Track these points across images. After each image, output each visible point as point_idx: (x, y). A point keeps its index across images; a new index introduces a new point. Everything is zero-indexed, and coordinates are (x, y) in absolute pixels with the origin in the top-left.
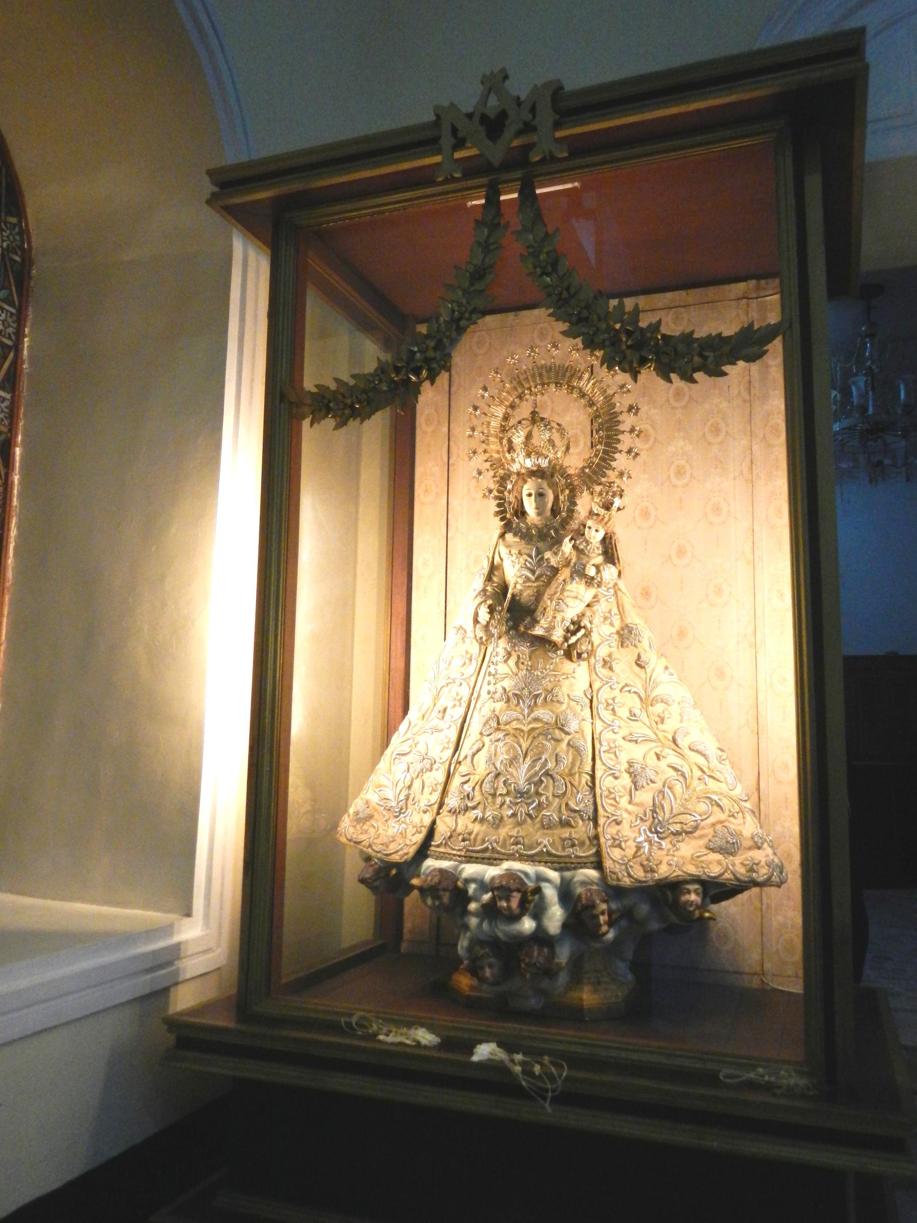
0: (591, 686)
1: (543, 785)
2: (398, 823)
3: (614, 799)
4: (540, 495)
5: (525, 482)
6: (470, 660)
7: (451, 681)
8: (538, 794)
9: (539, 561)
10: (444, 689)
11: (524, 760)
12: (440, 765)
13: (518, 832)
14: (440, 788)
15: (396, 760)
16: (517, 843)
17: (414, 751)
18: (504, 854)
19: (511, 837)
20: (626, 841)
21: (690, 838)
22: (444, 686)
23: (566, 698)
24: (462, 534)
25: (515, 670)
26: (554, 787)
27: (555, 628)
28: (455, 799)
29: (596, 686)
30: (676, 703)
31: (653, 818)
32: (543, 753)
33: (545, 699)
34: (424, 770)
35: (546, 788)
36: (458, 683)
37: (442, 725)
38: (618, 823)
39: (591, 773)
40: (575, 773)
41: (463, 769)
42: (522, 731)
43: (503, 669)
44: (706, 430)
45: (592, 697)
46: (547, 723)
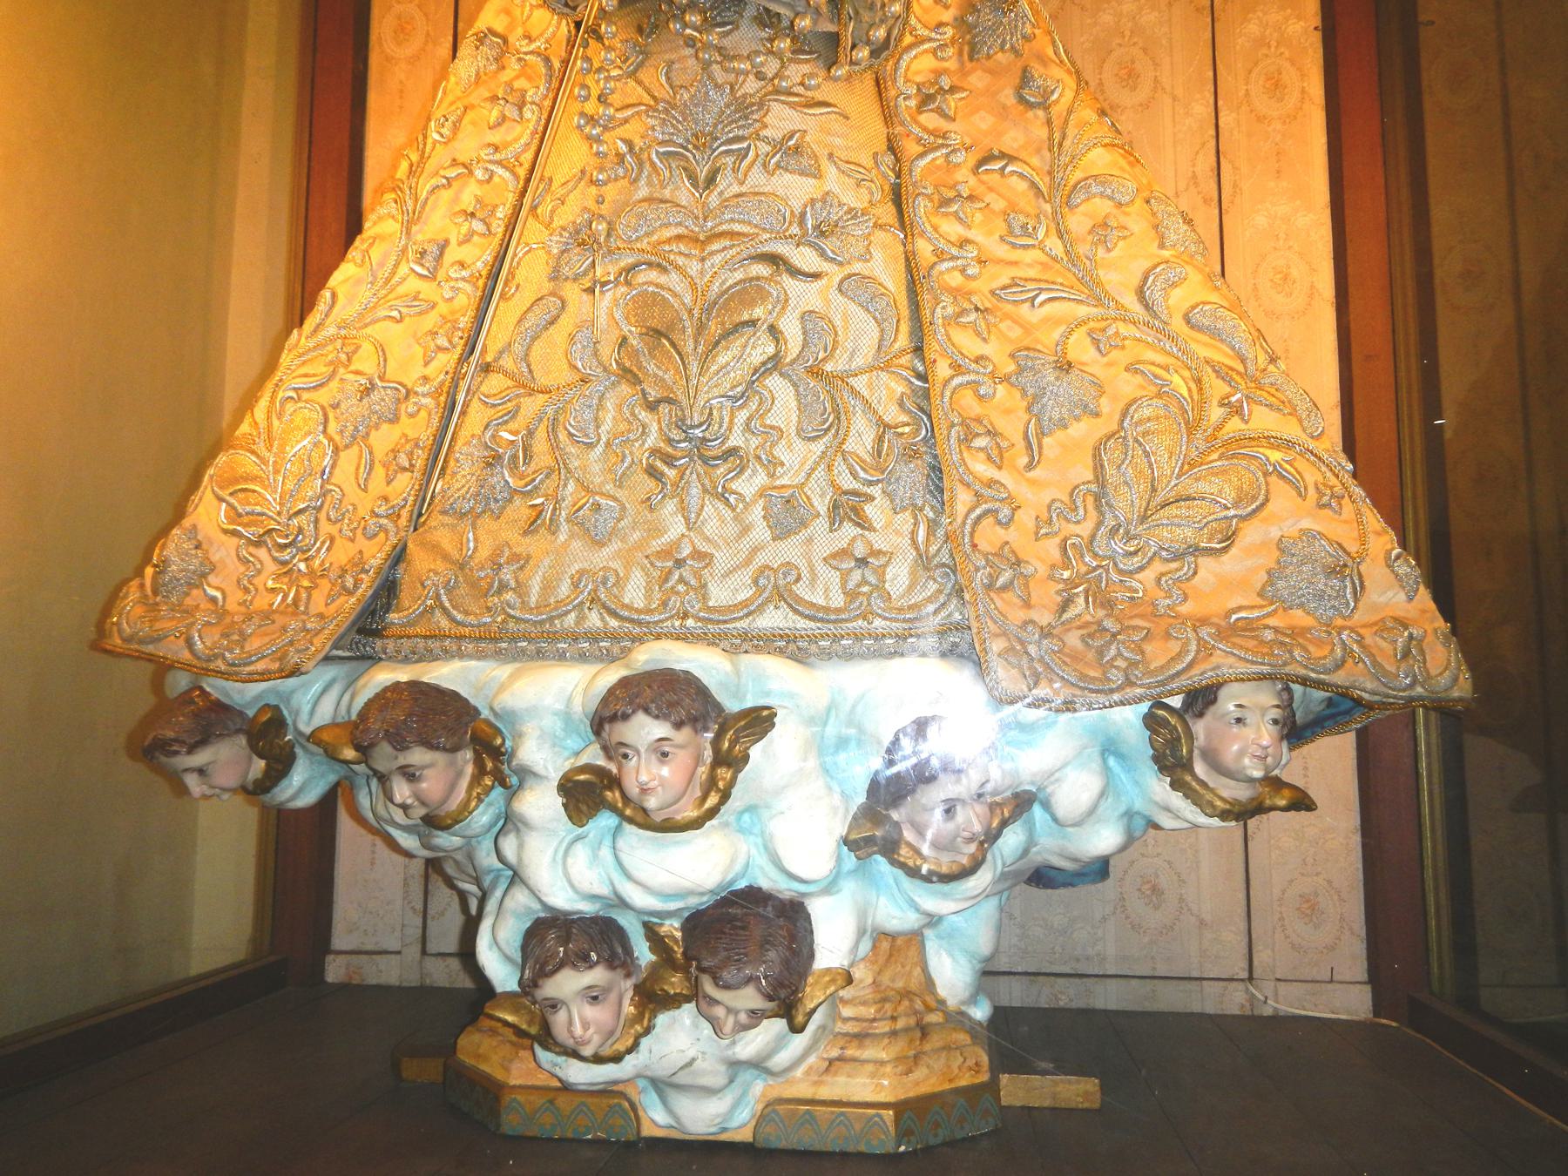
2: (286, 580)
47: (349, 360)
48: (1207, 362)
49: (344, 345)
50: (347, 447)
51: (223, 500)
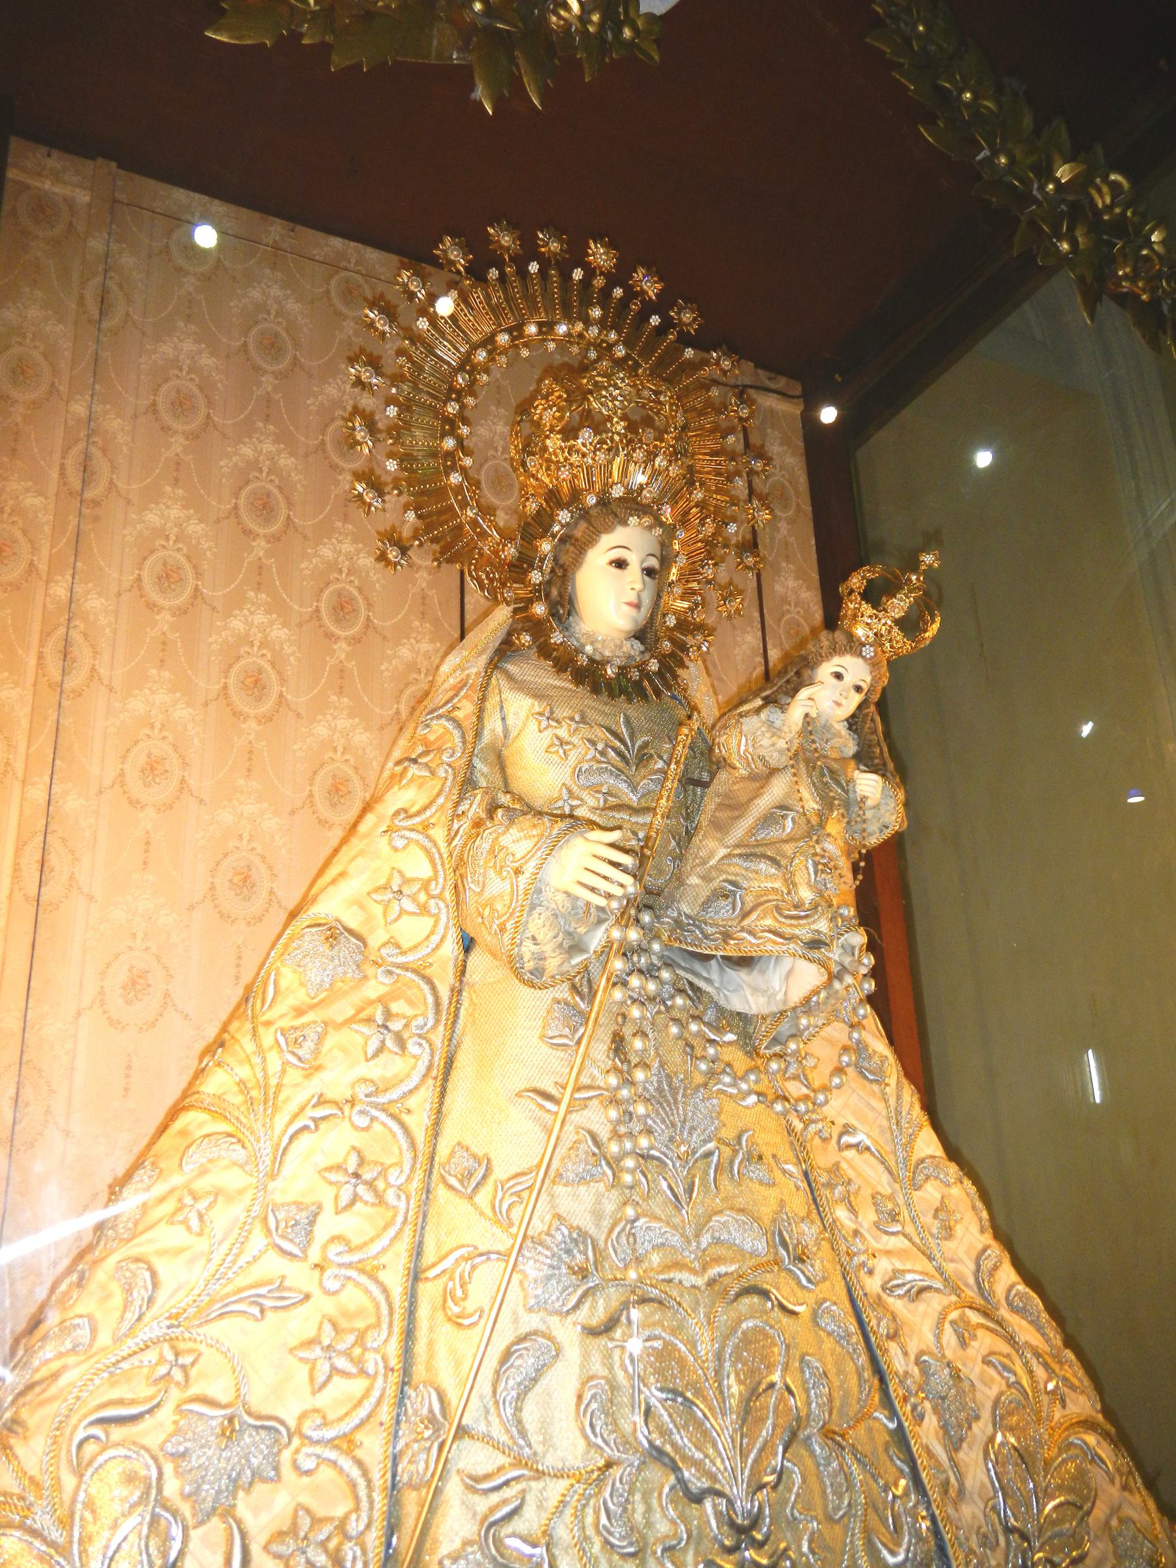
22: (305, 1128)
37: (299, 1276)
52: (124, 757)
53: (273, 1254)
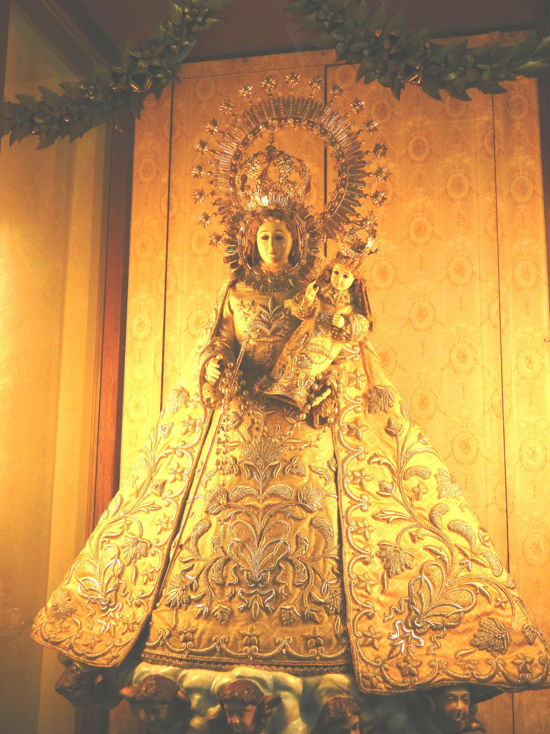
0: (335, 456)
1: (282, 572)
2: (105, 619)
3: (365, 588)
4: (278, 238)
5: (261, 223)
6: (194, 426)
7: (172, 451)
8: (276, 583)
9: (275, 313)
10: (163, 460)
11: (258, 544)
12: (156, 549)
13: (252, 629)
14: (157, 577)
15: (105, 544)
16: (250, 644)
17: (126, 533)
18: (235, 657)
19: (243, 636)
20: (379, 639)
21: (453, 633)
22: (162, 457)
23: (308, 470)
24: (182, 292)
25: (247, 437)
26: (294, 574)
27: (297, 387)
28: (175, 590)
29: (342, 455)
30: (432, 477)
31: (410, 610)
32: (281, 535)
33: (283, 470)
34: (138, 556)
35: (285, 575)
36: (179, 454)
37: (159, 501)
38: (370, 617)
39: (337, 557)
40: (319, 559)
41: (185, 554)
42: (257, 508)
43: (234, 436)
44: (449, 186)
45: (337, 469)
46: (285, 499)
47: (128, 528)
48: (456, 546)
49: (126, 521)
50: (128, 565)
51: (79, 582)
52: (188, 319)
53: (152, 494)
